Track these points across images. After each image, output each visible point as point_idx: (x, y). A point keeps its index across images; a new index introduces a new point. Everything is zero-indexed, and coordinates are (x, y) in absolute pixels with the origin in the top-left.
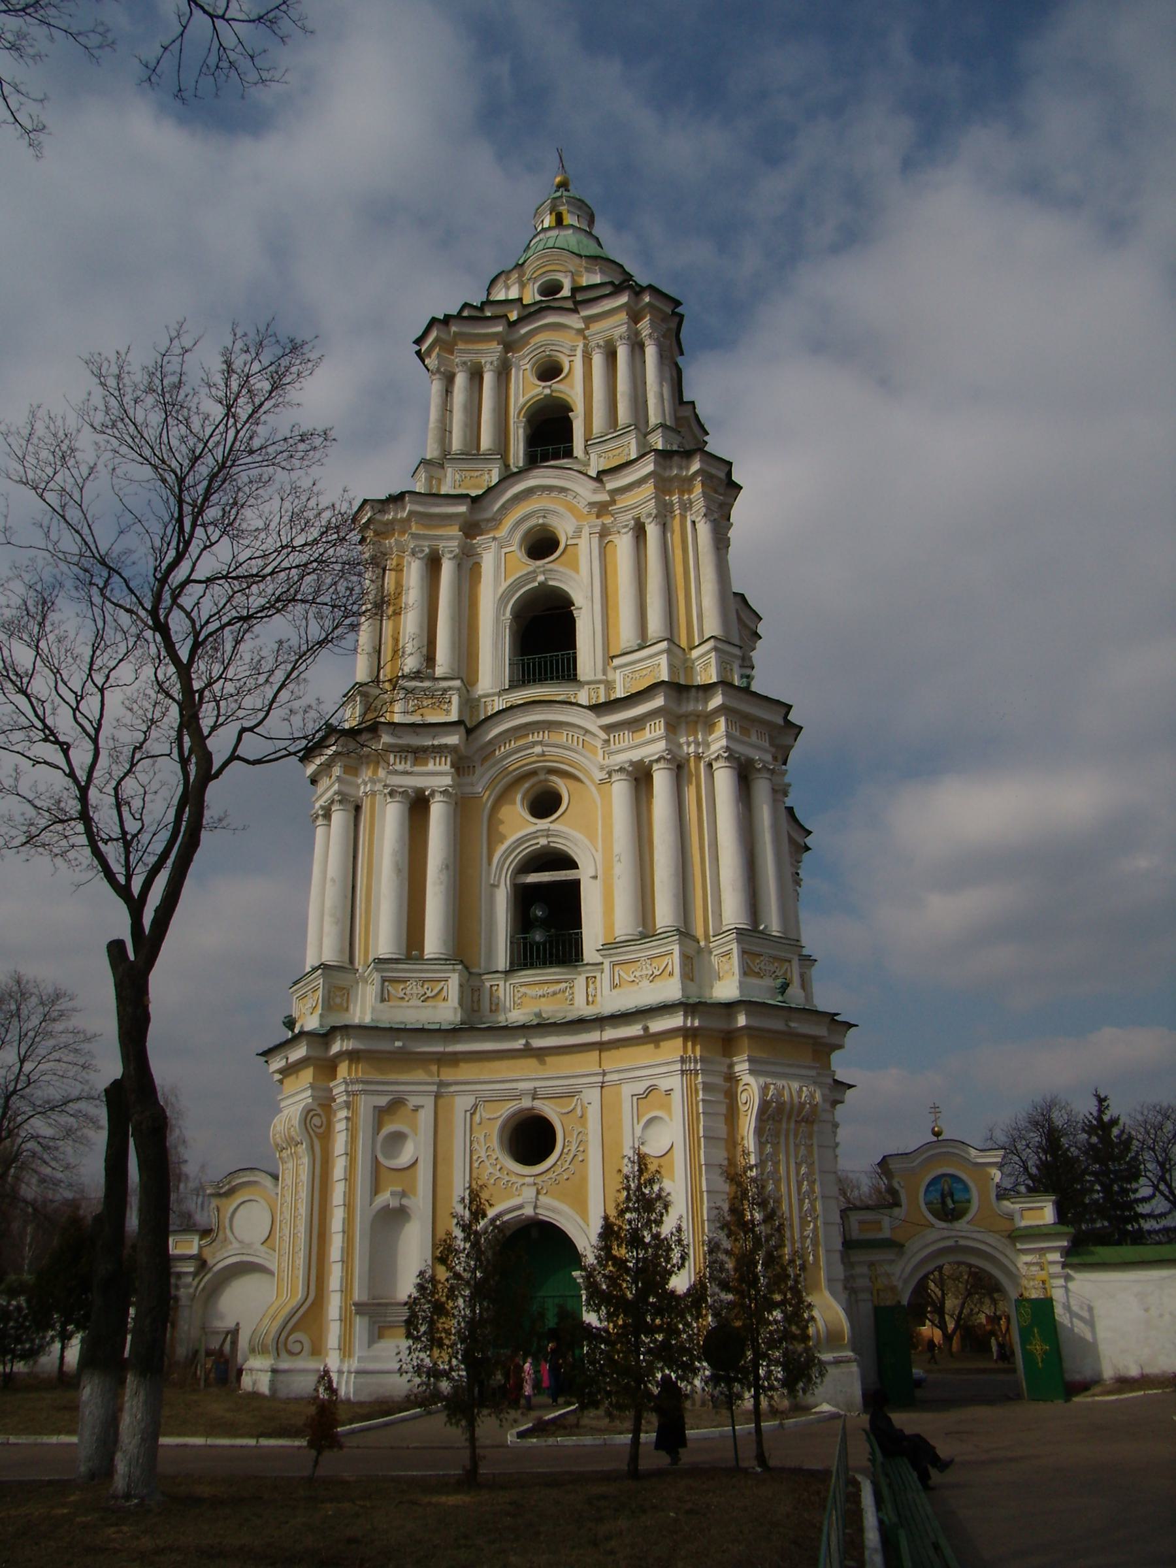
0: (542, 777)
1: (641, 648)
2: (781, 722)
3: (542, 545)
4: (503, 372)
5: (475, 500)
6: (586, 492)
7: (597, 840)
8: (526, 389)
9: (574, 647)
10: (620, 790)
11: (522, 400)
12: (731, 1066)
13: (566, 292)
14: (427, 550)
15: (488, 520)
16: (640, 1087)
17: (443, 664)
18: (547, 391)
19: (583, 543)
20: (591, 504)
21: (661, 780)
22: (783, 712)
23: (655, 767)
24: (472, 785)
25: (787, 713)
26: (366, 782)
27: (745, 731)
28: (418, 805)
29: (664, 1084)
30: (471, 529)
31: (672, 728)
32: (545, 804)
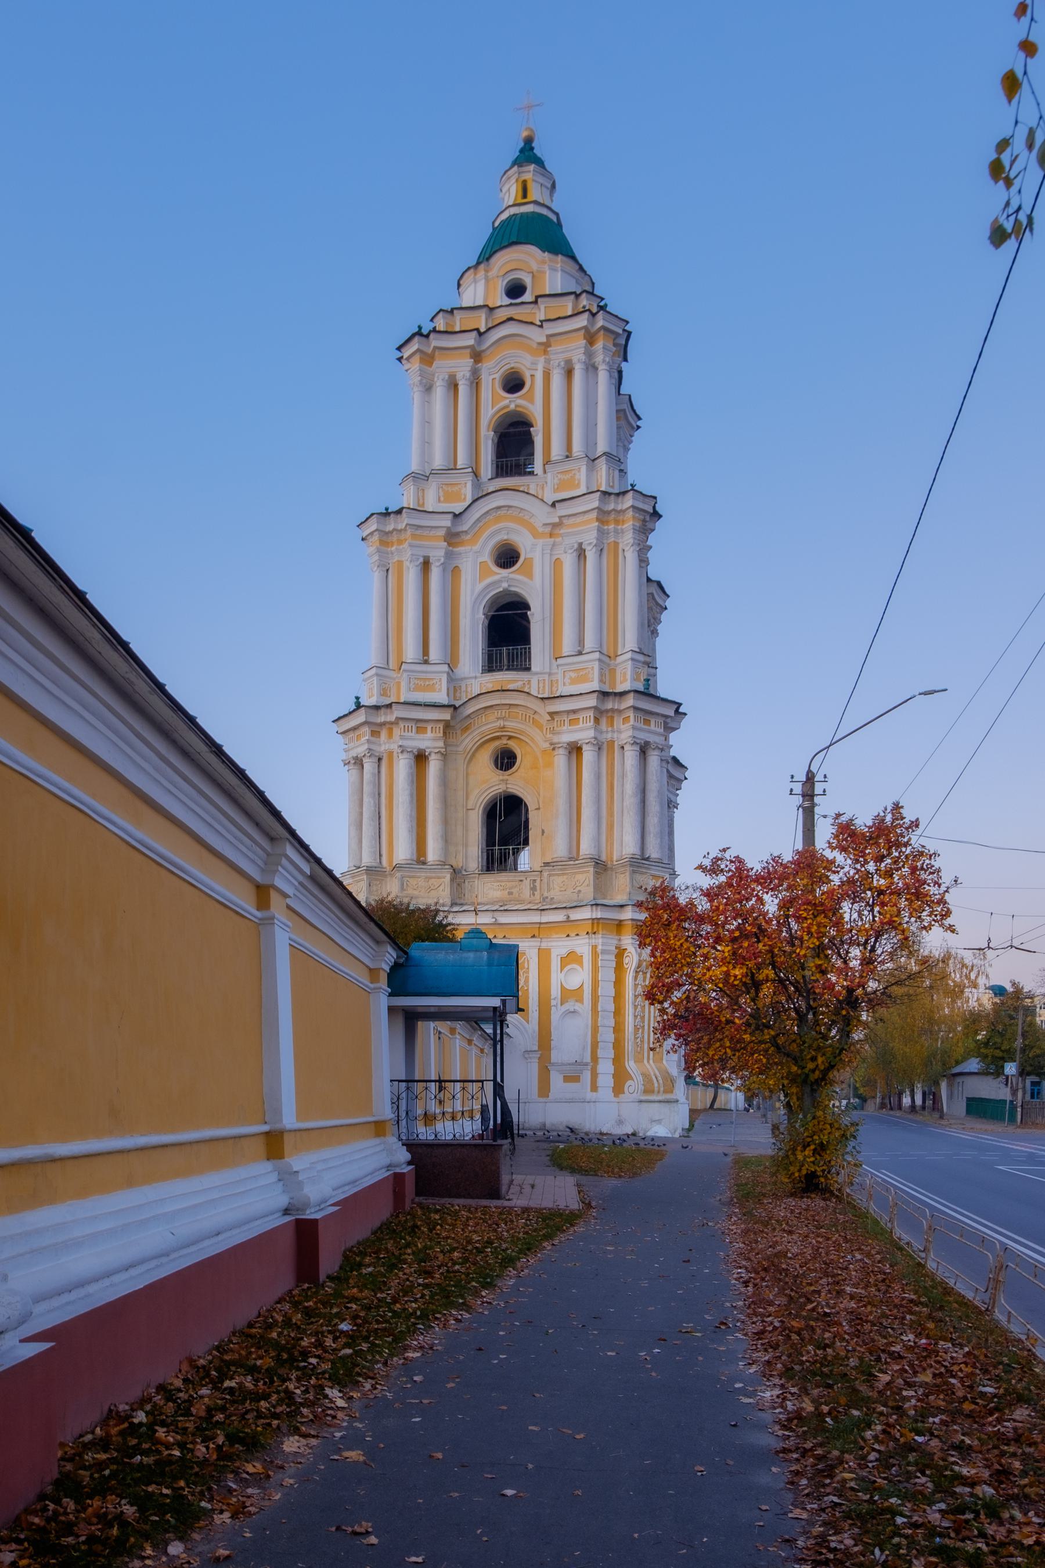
0: (505, 742)
1: (580, 653)
2: (672, 714)
3: (507, 557)
4: (475, 383)
5: (456, 516)
6: (542, 516)
7: (543, 786)
8: (495, 403)
9: (529, 644)
10: (560, 760)
11: (491, 412)
12: (620, 940)
13: (528, 297)
14: (421, 560)
15: (466, 532)
16: (564, 952)
17: (434, 655)
18: (512, 406)
19: (537, 557)
20: (545, 525)
21: (588, 755)
22: (676, 706)
23: (585, 748)
24: (457, 746)
25: (678, 709)
26: (385, 744)
27: (647, 722)
28: (421, 758)
29: (579, 950)
30: (452, 538)
31: (597, 720)
32: (506, 760)
